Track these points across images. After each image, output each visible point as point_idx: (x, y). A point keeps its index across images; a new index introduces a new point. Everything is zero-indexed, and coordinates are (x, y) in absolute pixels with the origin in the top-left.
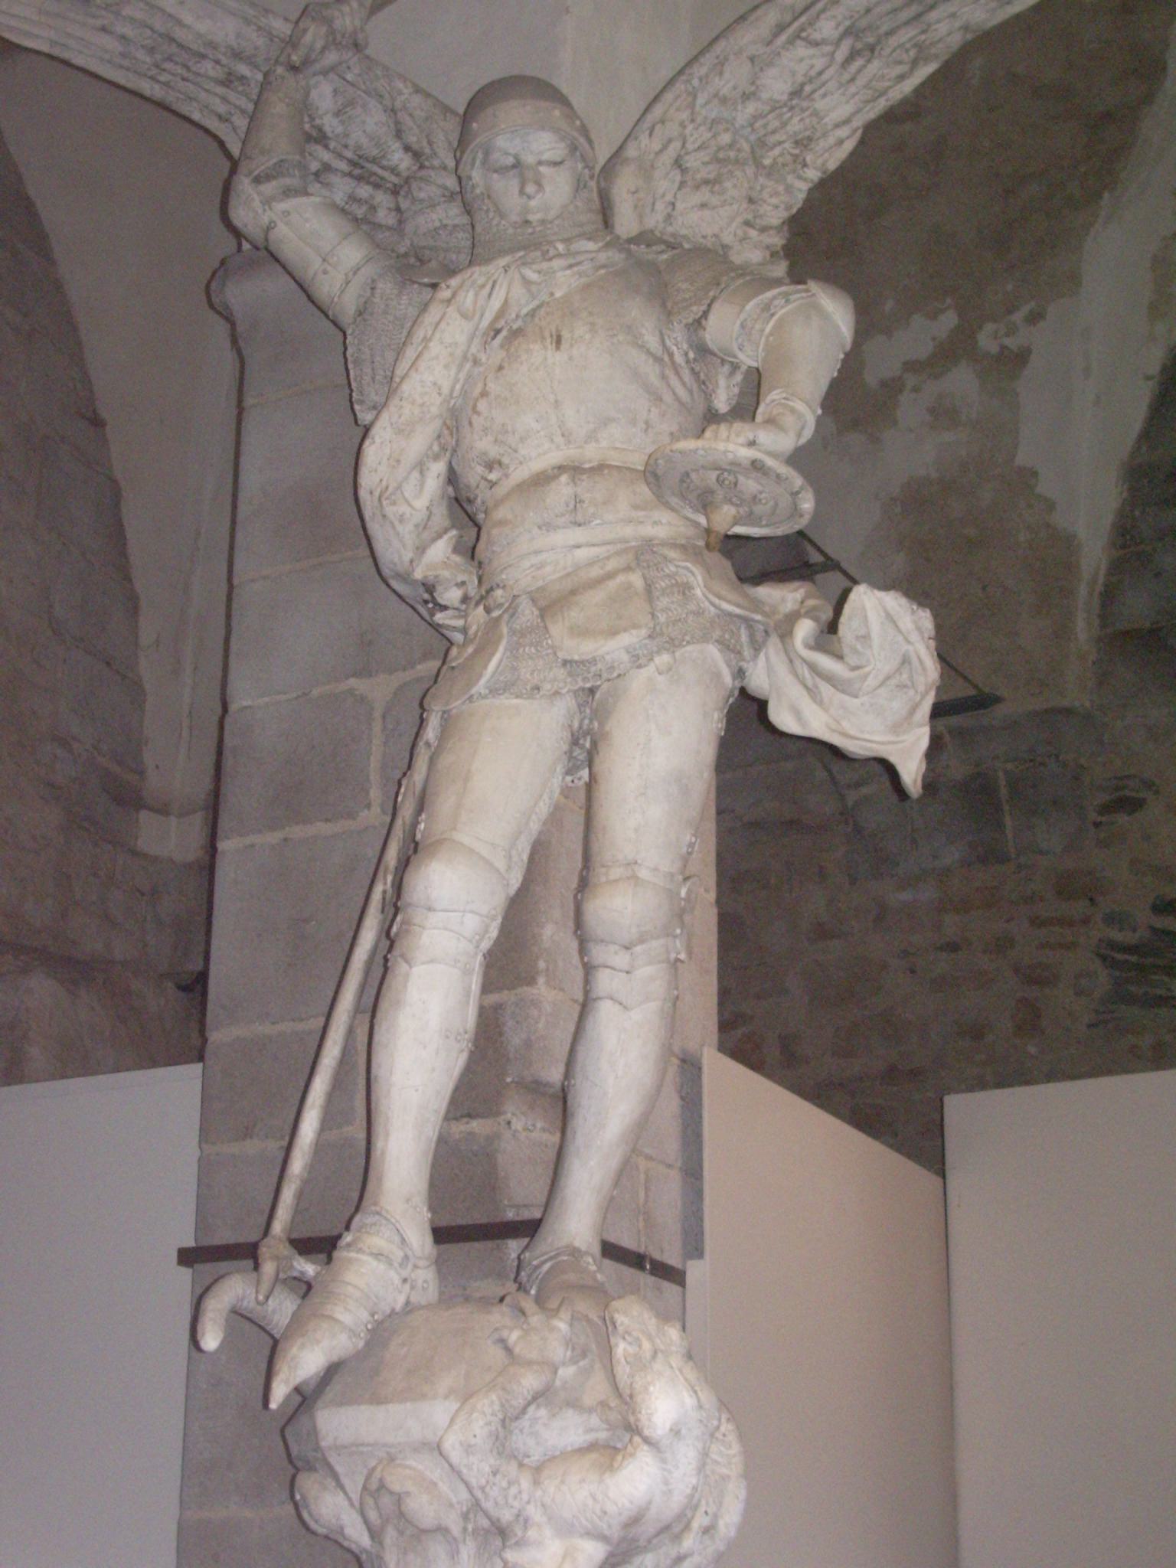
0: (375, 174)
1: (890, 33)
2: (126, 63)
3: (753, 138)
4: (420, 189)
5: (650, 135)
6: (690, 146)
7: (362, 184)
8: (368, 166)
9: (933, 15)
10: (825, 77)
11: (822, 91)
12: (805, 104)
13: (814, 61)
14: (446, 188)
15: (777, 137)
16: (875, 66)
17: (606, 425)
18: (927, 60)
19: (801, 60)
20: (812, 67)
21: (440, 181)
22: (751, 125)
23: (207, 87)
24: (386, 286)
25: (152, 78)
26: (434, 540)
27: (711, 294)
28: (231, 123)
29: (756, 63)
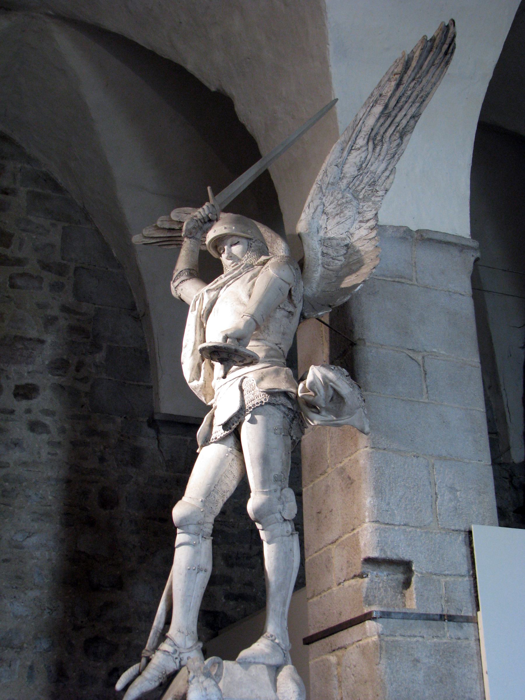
1: (386, 131)
6: (327, 205)
9: (398, 119)
11: (370, 164)
12: (365, 171)
15: (361, 186)
16: (385, 146)
19: (356, 157)
20: (361, 157)
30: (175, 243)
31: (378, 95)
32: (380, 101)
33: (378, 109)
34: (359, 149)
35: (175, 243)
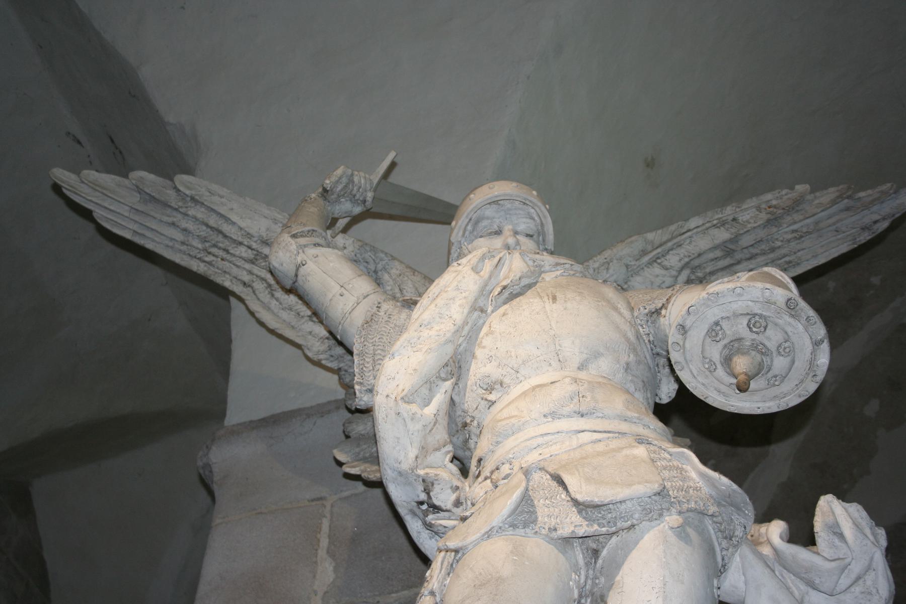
2: (184, 248)
13: (664, 279)
17: (596, 357)
19: (657, 276)
20: (664, 282)
23: (239, 264)
25: (200, 259)
28: (252, 288)
29: (630, 270)
30: (135, 227)
31: (731, 218)
32: (729, 226)
33: (722, 235)
35: (135, 227)
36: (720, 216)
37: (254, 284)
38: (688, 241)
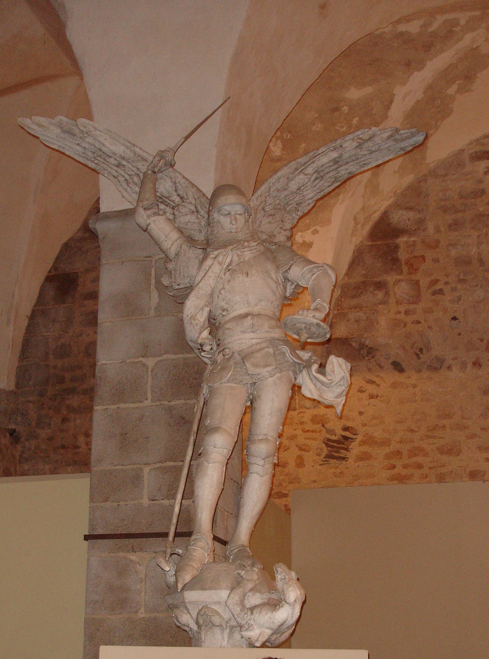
0: (167, 202)
1: (328, 173)
2: (83, 155)
3: (285, 202)
4: (182, 209)
5: (257, 200)
6: (267, 204)
7: (162, 204)
8: (165, 199)
10: (307, 184)
12: (301, 193)
14: (191, 209)
15: (291, 202)
16: (322, 182)
18: (337, 182)
21: (189, 207)
22: (285, 198)
24: (185, 247)
25: (92, 161)
26: (205, 330)
27: (291, 262)
31: (340, 144)
33: (335, 155)
34: (307, 175)
36: (334, 145)
37: (119, 178)
38: (318, 159)
